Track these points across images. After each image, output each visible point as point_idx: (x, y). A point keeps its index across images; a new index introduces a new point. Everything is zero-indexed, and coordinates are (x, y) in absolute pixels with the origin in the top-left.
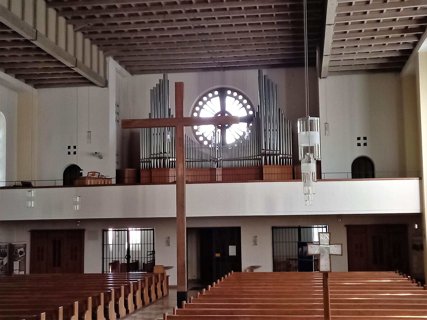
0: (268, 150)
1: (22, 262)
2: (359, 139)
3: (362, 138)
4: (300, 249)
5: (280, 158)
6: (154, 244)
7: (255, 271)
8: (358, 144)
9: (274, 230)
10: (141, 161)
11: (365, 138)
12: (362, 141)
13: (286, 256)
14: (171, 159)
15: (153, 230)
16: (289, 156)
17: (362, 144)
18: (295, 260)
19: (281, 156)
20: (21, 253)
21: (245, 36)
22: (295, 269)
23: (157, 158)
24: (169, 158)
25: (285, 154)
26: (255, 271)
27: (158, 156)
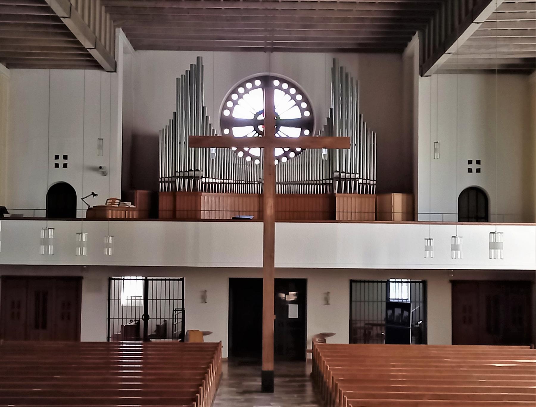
0: (338, 172)
2: (470, 162)
3: (474, 162)
4: (390, 312)
6: (183, 300)
7: (329, 341)
8: (469, 169)
9: (354, 284)
10: (160, 180)
11: (478, 162)
12: (474, 166)
13: (365, 321)
14: (204, 180)
15: (182, 280)
16: (372, 182)
17: (474, 170)
18: (381, 325)
19: (361, 181)
21: (329, 15)
22: (378, 339)
23: (185, 178)
24: (202, 177)
25: (367, 179)
26: (329, 341)
27: (187, 174)
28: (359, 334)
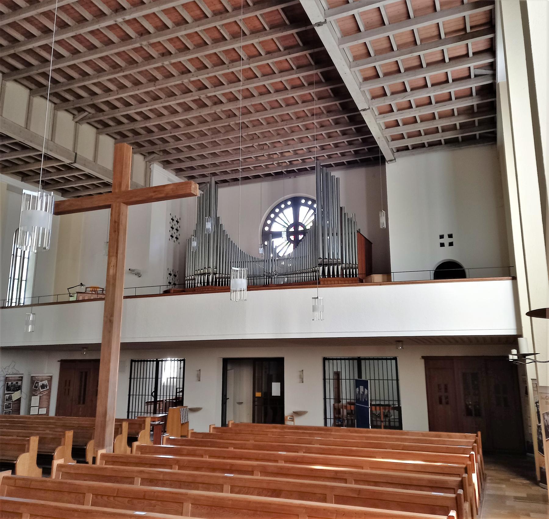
1: (45, 397)
2: (442, 237)
3: (446, 237)
4: (357, 389)
5: (342, 268)
9: (327, 362)
11: (450, 236)
12: (446, 240)
15: (184, 360)
17: (446, 244)
20: (43, 386)
23: (201, 274)
28: (348, 414)
